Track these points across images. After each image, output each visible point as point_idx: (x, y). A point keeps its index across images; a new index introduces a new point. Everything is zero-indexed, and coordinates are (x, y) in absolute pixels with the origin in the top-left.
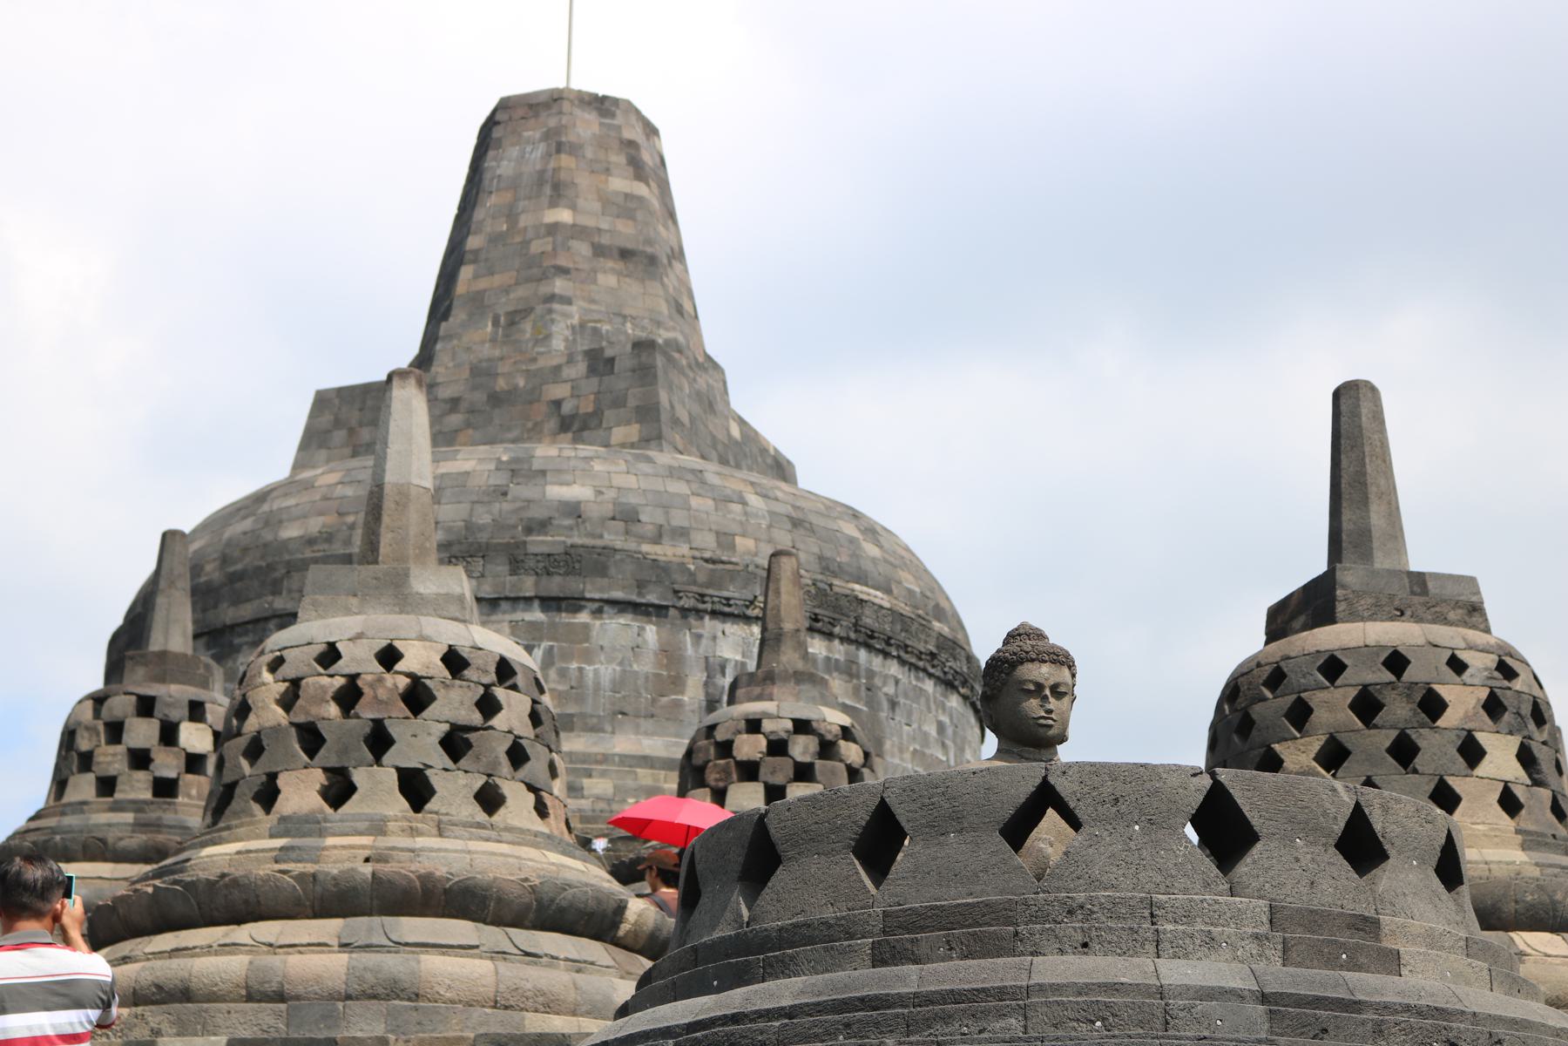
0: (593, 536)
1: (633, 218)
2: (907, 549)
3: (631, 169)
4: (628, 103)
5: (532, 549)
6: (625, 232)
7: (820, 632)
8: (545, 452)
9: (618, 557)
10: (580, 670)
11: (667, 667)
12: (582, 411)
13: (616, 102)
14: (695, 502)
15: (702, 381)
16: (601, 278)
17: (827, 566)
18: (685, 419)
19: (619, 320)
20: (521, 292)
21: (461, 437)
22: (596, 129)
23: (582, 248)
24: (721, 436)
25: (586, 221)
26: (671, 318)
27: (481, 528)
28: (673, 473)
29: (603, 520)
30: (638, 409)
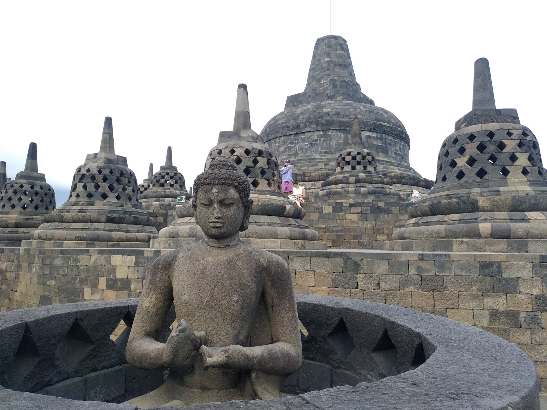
0: (331, 118)
1: (342, 58)
2: (393, 115)
5: (320, 121)
6: (340, 61)
7: (375, 132)
8: (322, 103)
9: (336, 121)
15: (354, 88)
16: (336, 70)
17: (376, 119)
19: (339, 77)
20: (321, 75)
23: (332, 65)
24: (359, 97)
25: (333, 60)
26: (349, 76)
27: (311, 118)
28: (347, 105)
29: (333, 115)
30: (342, 93)
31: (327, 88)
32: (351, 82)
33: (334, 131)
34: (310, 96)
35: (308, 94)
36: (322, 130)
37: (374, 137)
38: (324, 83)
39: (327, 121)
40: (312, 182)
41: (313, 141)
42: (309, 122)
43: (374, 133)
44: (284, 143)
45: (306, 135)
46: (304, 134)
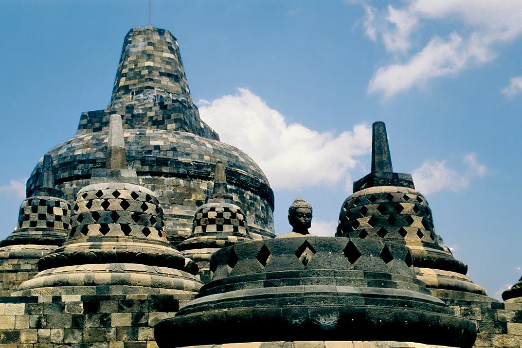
1: (170, 64)
3: (169, 51)
12: (158, 120)
14: (192, 146)
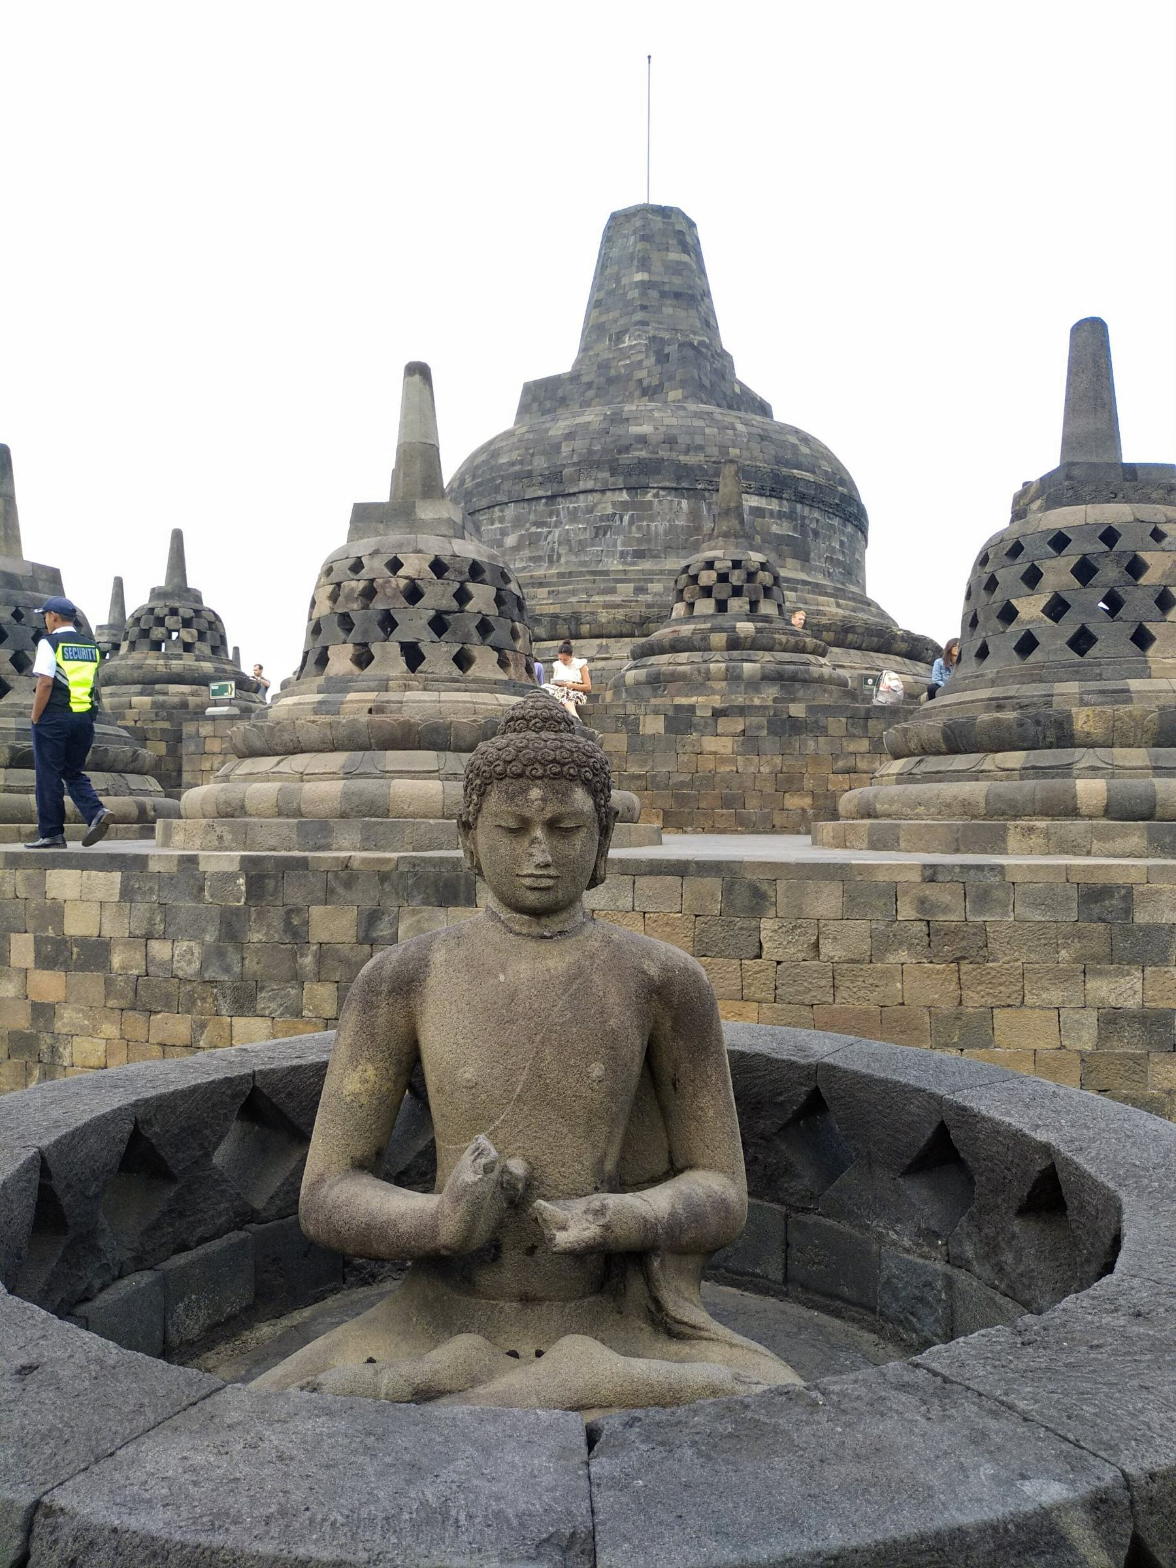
0: (653, 453)
2: (826, 448)
4: (678, 209)
5: (621, 462)
7: (775, 497)
8: (629, 408)
10: (648, 525)
11: (693, 521)
12: (653, 384)
13: (671, 209)
14: (707, 430)
15: (717, 365)
16: (664, 309)
17: (778, 461)
18: (708, 386)
19: (674, 332)
20: (622, 322)
21: (594, 402)
22: (661, 226)
23: (654, 294)
25: (658, 279)
26: (702, 329)
28: (697, 415)
29: (658, 445)
30: (681, 381)
31: (641, 362)
32: (707, 347)
33: (662, 493)
34: (590, 385)
35: (585, 379)
36: (627, 489)
37: (771, 512)
38: (631, 347)
39: (641, 461)
40: (598, 641)
41: (602, 518)
42: (589, 463)
43: (773, 499)
44: (518, 523)
45: (582, 502)
46: (574, 499)
